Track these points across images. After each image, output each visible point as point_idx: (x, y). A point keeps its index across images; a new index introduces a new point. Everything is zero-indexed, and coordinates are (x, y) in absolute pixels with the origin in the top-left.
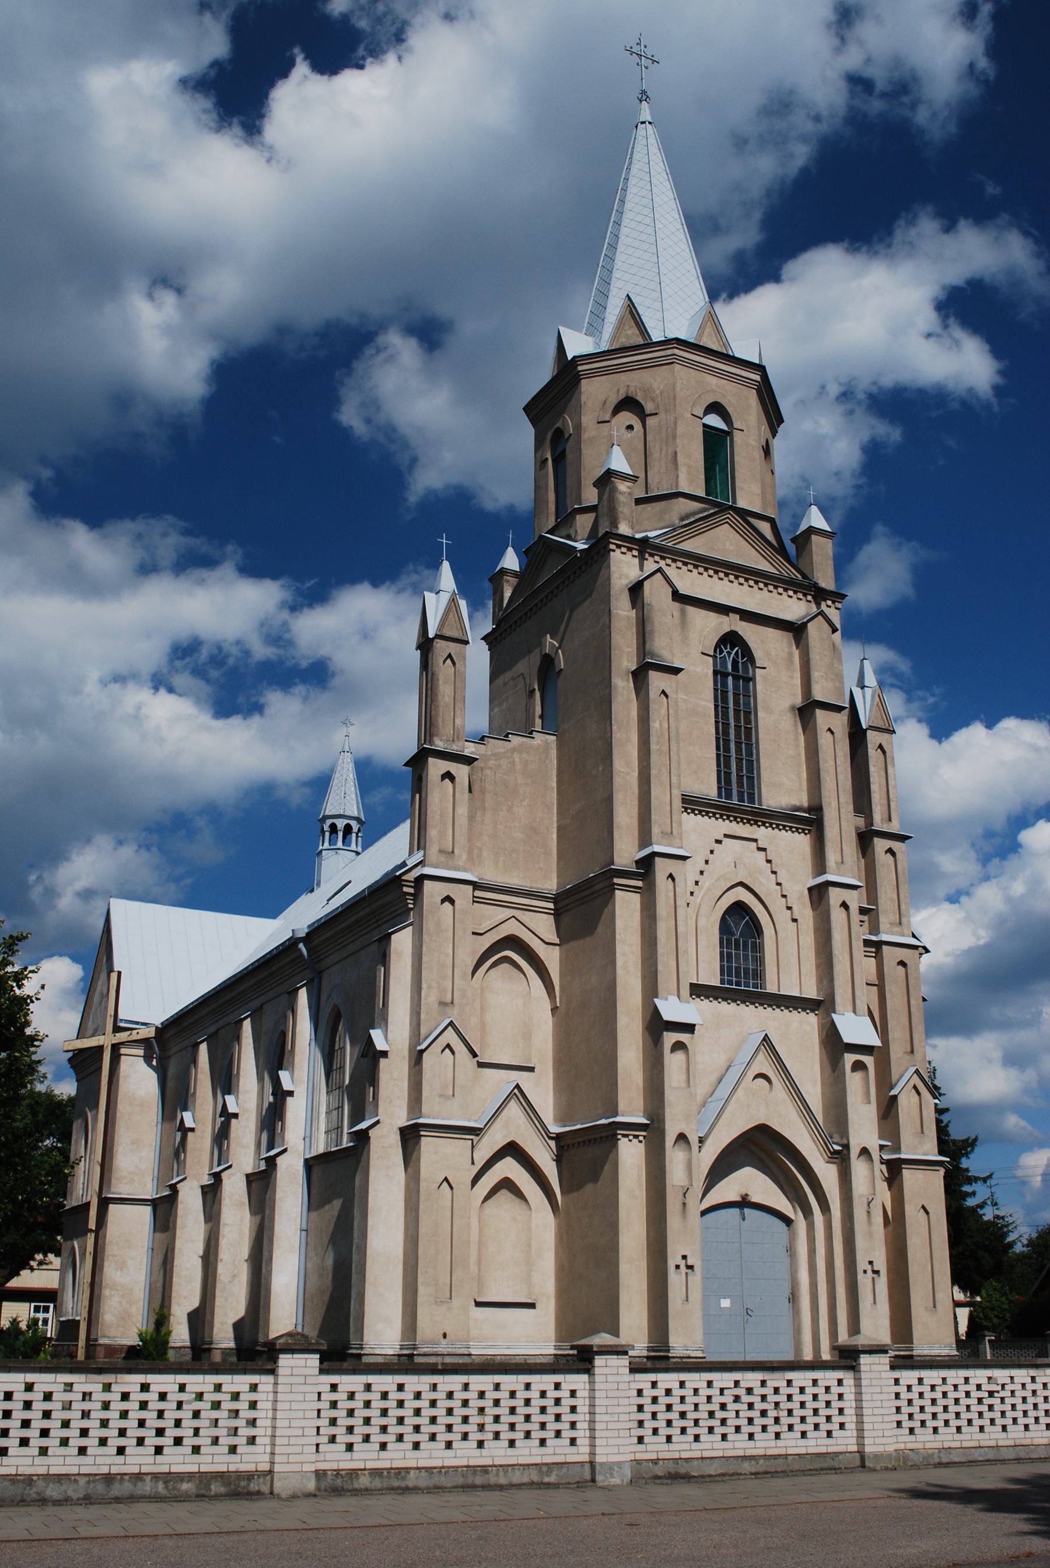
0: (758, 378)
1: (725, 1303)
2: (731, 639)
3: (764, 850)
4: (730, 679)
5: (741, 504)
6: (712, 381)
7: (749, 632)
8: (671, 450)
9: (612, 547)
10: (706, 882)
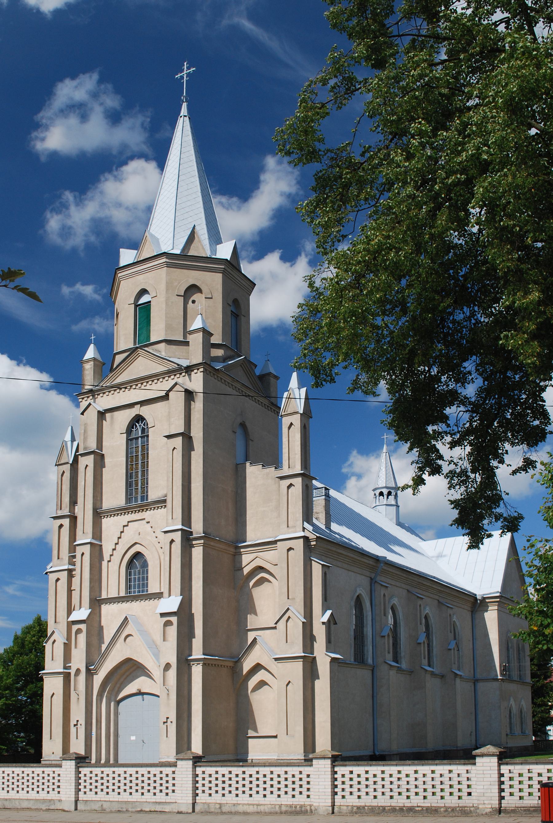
0: (164, 260)
1: (133, 738)
2: (139, 419)
6: (140, 278)
7: (144, 411)
9: (80, 400)
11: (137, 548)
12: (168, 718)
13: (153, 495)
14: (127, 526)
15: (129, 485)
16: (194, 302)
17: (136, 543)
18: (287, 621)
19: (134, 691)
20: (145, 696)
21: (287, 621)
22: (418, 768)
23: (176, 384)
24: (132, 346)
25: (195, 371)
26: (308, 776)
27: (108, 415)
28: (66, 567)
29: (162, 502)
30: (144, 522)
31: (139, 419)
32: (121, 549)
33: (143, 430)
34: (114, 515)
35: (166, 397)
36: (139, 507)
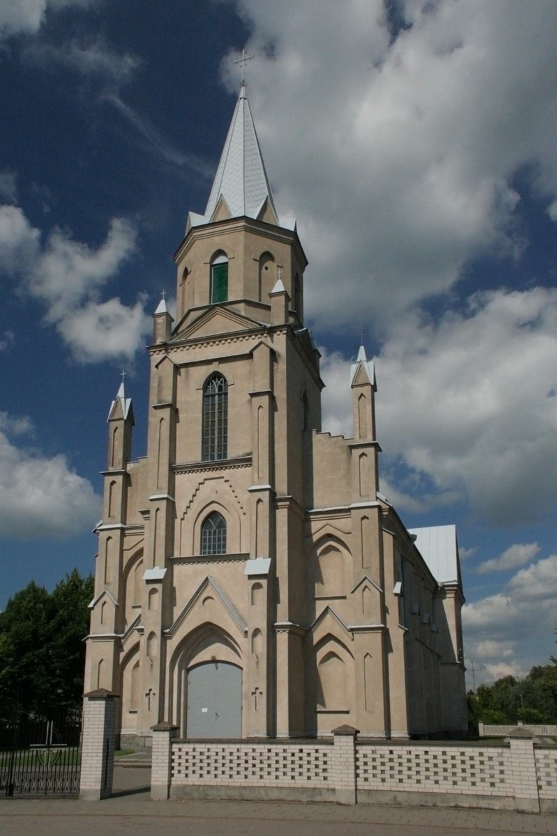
1: (205, 710)
2: (216, 376)
3: (228, 481)
4: (217, 397)
6: (217, 239)
7: (223, 368)
10: (194, 506)
11: (214, 507)
12: (257, 688)
13: (233, 453)
15: (204, 442)
16: (266, 268)
17: (213, 502)
18: (364, 590)
20: (219, 664)
21: (364, 590)
22: (446, 749)
23: (261, 343)
24: (207, 304)
26: (325, 755)
27: (183, 370)
28: (119, 525)
29: (246, 461)
30: (223, 480)
31: (216, 376)
32: (196, 507)
33: (220, 388)
35: (250, 356)
36: (218, 464)
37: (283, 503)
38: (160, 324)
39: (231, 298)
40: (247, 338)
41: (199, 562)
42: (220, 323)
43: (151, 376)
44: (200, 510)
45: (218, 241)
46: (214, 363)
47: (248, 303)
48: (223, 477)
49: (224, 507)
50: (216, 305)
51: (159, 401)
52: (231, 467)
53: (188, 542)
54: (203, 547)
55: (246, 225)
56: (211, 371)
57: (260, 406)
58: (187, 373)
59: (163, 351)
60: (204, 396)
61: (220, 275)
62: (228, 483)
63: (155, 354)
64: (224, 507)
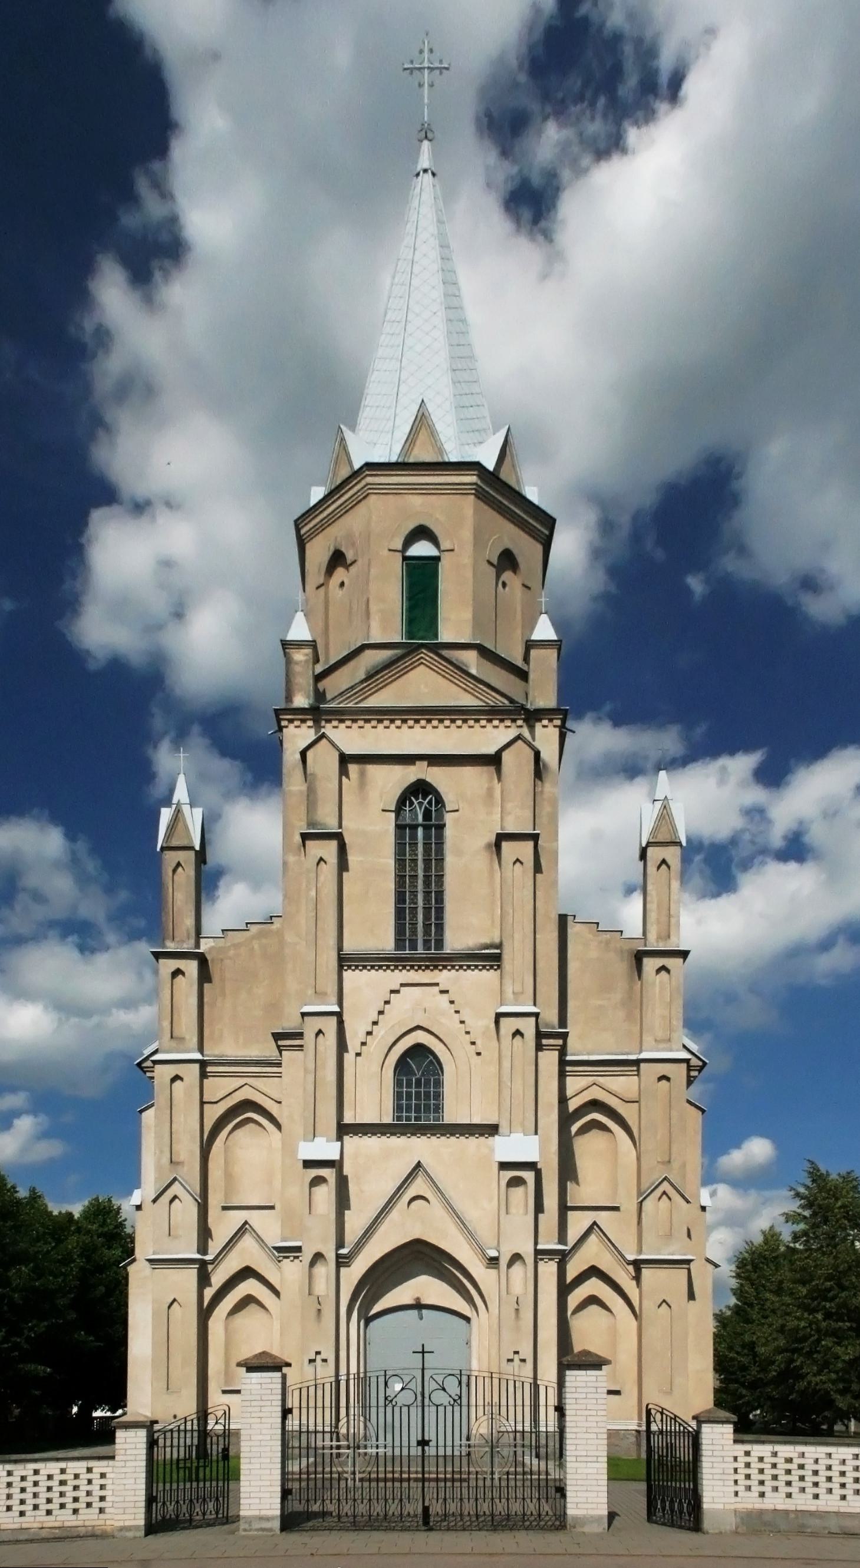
0: (474, 479)
2: (421, 789)
3: (447, 992)
4: (420, 831)
5: (446, 634)
6: (416, 501)
7: (436, 776)
8: (365, 599)
13: (455, 940)
14: (397, 992)
15: (400, 914)
19: (408, 1300)
20: (424, 1312)
24: (397, 639)
25: (545, 722)
28: (198, 1056)
29: (490, 958)
30: (436, 989)
31: (421, 789)
32: (384, 1034)
33: (427, 815)
34: (357, 967)
35: (494, 761)
36: (430, 959)
37: (552, 1041)
38: (297, 663)
39: (446, 634)
40: (483, 723)
41: (393, 1134)
42: (423, 684)
43: (285, 771)
44: (394, 1040)
45: (421, 508)
46: (418, 763)
47: (484, 652)
48: (437, 984)
49: (441, 1040)
50: (423, 646)
51: (311, 824)
52: (453, 967)
53: (373, 1097)
54: (398, 1108)
55: (479, 482)
56: (413, 779)
57: (518, 860)
58: (362, 774)
59: (310, 723)
60: (397, 825)
61: (421, 582)
62: (445, 996)
63: (291, 726)
64: (441, 1040)
